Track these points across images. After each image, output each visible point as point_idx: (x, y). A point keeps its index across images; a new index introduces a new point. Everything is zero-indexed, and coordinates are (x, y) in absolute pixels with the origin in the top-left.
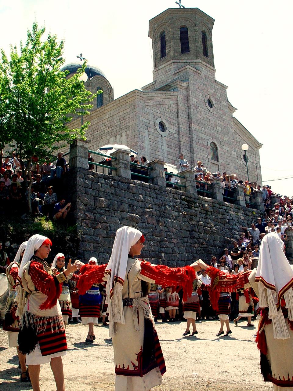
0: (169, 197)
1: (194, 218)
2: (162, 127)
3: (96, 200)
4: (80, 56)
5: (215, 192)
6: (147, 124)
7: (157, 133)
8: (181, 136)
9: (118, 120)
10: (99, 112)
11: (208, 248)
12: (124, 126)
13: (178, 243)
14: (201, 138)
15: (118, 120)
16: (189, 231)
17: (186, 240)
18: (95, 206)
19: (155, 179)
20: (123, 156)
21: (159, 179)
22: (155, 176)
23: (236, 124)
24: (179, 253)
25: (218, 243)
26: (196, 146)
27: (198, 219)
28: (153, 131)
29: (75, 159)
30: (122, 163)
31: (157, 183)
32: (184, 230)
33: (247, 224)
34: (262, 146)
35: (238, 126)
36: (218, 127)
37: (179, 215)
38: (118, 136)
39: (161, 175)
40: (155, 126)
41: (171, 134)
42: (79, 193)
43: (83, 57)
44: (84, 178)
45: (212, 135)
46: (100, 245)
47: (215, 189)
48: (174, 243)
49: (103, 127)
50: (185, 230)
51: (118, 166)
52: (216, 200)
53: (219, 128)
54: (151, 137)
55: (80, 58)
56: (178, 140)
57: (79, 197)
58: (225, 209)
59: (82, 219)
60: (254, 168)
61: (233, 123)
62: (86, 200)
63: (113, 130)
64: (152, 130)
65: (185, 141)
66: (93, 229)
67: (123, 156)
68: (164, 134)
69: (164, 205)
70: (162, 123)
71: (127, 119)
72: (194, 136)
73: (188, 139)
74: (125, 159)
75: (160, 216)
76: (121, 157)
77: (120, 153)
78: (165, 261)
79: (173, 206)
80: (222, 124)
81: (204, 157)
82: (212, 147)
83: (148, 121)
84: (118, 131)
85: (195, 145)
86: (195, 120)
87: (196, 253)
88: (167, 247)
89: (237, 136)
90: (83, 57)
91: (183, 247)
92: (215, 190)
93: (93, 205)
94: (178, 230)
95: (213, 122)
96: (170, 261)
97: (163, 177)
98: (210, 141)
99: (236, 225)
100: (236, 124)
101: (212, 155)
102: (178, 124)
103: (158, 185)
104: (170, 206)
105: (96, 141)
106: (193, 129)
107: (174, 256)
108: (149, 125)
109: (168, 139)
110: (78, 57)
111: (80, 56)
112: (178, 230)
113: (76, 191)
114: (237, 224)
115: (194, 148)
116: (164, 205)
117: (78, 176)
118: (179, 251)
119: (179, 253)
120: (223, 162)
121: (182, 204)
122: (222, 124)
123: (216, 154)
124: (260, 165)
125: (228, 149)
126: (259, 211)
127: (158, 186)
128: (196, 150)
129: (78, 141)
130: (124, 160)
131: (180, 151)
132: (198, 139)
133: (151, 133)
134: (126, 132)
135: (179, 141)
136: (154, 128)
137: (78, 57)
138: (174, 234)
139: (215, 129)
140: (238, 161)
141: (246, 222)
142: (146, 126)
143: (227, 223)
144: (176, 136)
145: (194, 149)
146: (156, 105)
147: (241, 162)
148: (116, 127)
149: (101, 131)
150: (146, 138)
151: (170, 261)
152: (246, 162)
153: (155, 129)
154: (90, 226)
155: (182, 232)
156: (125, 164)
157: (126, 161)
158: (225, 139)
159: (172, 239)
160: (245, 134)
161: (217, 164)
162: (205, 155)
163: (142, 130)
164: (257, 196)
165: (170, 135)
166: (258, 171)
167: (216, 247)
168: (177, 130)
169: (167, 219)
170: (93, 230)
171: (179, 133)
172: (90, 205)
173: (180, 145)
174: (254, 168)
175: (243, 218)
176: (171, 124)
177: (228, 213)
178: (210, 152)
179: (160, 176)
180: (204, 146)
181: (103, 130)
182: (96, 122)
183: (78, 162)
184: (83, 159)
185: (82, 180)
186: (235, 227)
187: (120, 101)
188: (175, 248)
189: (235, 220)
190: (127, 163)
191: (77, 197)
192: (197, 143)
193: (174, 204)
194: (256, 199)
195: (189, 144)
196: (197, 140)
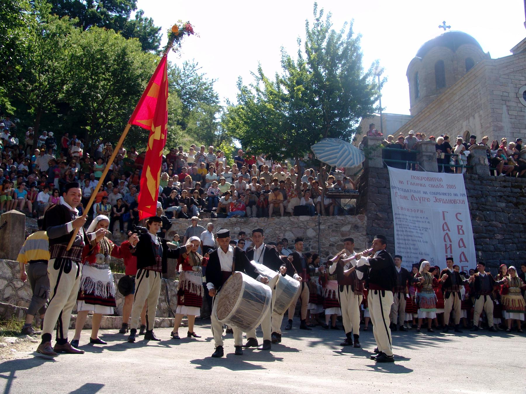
0: (494, 186)
4: (442, 25)
7: (522, 106)
9: (470, 100)
10: (448, 94)
13: (504, 239)
15: (470, 100)
17: (517, 235)
19: (474, 167)
21: (478, 168)
22: (474, 165)
24: (505, 251)
28: (515, 105)
30: (425, 155)
31: (476, 171)
32: (516, 223)
37: (507, 206)
38: (471, 119)
39: (482, 162)
43: (447, 25)
48: (498, 239)
49: (455, 111)
50: (517, 223)
55: (442, 27)
64: (513, 104)
69: (484, 196)
71: (479, 97)
74: (429, 151)
75: (478, 209)
76: (424, 149)
77: (423, 145)
78: (482, 260)
79: (499, 196)
83: (505, 94)
88: (487, 244)
90: (447, 25)
91: (513, 243)
94: (506, 224)
96: (490, 261)
97: (485, 165)
103: (476, 174)
104: (495, 197)
105: (449, 128)
107: (498, 254)
110: (440, 27)
111: (442, 25)
112: (506, 224)
116: (484, 196)
118: (505, 249)
119: (505, 251)
129: (369, 141)
130: (429, 152)
134: (479, 112)
137: (440, 27)
142: (503, 100)
146: (518, 71)
149: (453, 116)
150: (503, 115)
151: (490, 261)
153: (517, 102)
154: (382, 227)
156: (430, 156)
157: (430, 152)
159: (495, 235)
181: (455, 114)
182: (447, 106)
185: (374, 180)
187: (469, 77)
190: (432, 154)
193: (502, 194)
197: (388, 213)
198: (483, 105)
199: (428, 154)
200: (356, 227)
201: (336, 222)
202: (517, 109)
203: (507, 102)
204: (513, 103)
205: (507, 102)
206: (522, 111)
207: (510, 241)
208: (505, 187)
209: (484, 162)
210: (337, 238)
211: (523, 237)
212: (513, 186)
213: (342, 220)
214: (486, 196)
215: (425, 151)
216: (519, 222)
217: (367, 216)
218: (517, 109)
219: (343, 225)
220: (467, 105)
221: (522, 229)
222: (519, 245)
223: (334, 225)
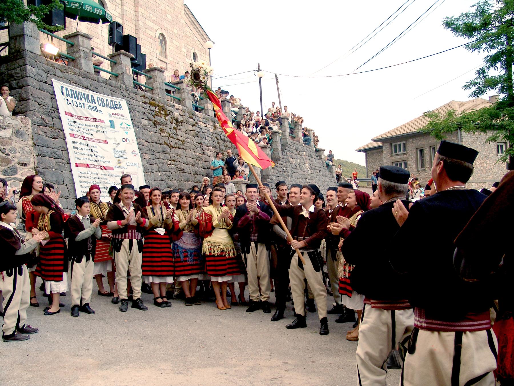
1: (165, 128)
3: (53, 100)
5: (183, 97)
11: (180, 166)
14: (148, 27)
16: (160, 144)
17: (158, 155)
18: (52, 107)
19: (120, 77)
20: (83, 41)
21: (125, 77)
25: (190, 160)
26: (143, 36)
27: (169, 130)
29: (22, 38)
31: (123, 81)
36: (168, 16)
39: (128, 72)
45: (161, 24)
46: (63, 161)
47: (184, 94)
50: (156, 143)
51: (76, 55)
52: (185, 108)
57: (32, 95)
58: (195, 119)
59: (38, 125)
61: (183, 12)
66: (53, 138)
67: (83, 41)
69: (132, 110)
72: (141, 23)
73: (133, 26)
74: (85, 46)
76: (81, 42)
77: (79, 37)
80: (172, 11)
81: (151, 52)
87: (169, 172)
89: (188, 29)
92: (183, 95)
95: (162, 8)
97: (130, 75)
98: (159, 32)
100: (187, 14)
101: (159, 49)
102: (122, 5)
103: (125, 85)
106: (140, 14)
114: (207, 137)
115: (140, 39)
120: (172, 59)
121: (152, 111)
122: (172, 11)
123: (164, 49)
125: (178, 44)
127: (125, 86)
130: (85, 47)
138: (146, 147)
139: (164, 17)
140: (187, 60)
141: (214, 135)
143: (198, 136)
145: (141, 40)
155: (154, 145)
157: (87, 48)
158: (175, 31)
159: (144, 154)
164: (225, 105)
167: (189, 165)
168: (121, 13)
169: (137, 129)
175: (212, 130)
176: (112, 3)
179: (126, 73)
180: (151, 38)
185: (34, 69)
188: (147, 165)
190: (88, 51)
193: (142, 110)
195: (135, 32)
196: (144, 29)
197: (53, 118)
199: (85, 49)
200: (18, 133)
207: (153, 161)
208: (145, 103)
209: (130, 72)
211: (162, 158)
212: (150, 104)
215: (82, 45)
216: (158, 142)
217: (32, 120)
221: (160, 150)
222: (160, 166)
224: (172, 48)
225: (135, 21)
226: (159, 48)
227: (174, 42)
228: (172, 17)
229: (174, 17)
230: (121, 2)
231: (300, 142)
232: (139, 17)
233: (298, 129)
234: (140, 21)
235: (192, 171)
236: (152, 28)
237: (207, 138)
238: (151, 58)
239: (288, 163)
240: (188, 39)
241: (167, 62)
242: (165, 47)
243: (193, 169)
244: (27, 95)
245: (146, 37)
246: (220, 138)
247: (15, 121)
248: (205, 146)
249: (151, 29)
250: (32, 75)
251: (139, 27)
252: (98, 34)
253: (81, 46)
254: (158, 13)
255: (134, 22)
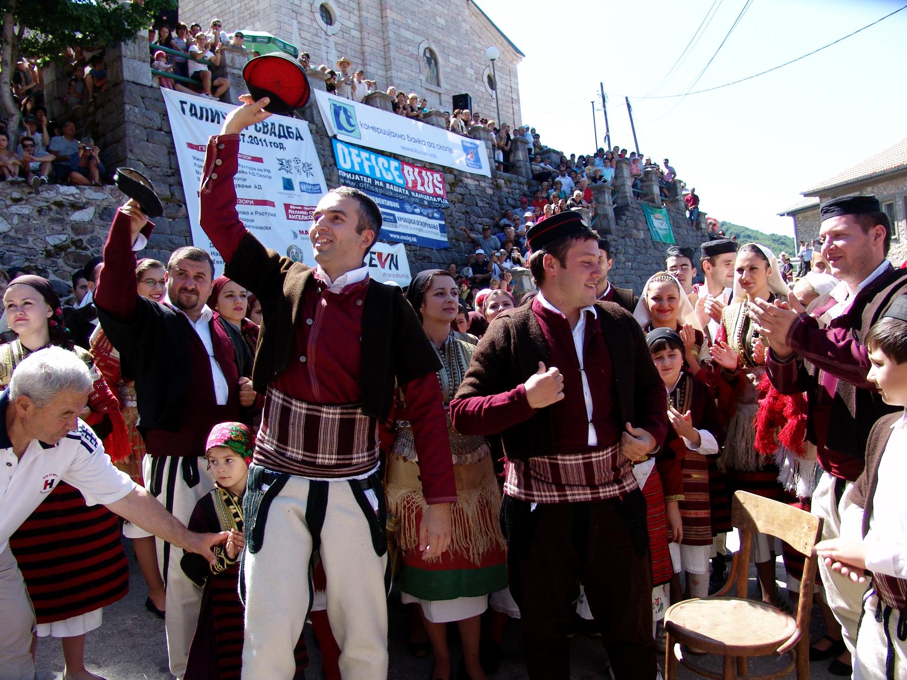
2: (327, 14)
3: (172, 157)
6: (296, 8)
7: (316, 26)
8: (366, 35)
12: (249, 12)
14: (405, 39)
23: (473, 14)
26: (397, 54)
28: (308, 23)
33: (499, 203)
34: (523, 59)
35: (476, 17)
36: (438, 19)
40: (311, 11)
41: (345, 31)
42: (132, 140)
44: (143, 105)
45: (427, 34)
53: (441, 21)
54: (304, 34)
56: (360, 43)
60: (508, 101)
62: (151, 156)
63: (227, 22)
64: (306, 21)
65: (373, 45)
67: (233, 60)
68: (330, 29)
69: (328, 165)
70: (326, 6)
72: (391, 35)
73: (379, 41)
77: (226, 52)
80: (446, 12)
82: (427, 58)
84: (237, 22)
85: (393, 53)
86: (393, 4)
89: (476, 38)
93: (168, 165)
95: (428, 8)
98: (424, 46)
99: (477, 205)
106: (390, 20)
108: (300, 11)
109: (340, 41)
113: (125, 135)
115: (392, 58)
116: (328, 165)
117: (126, 100)
120: (448, 87)
122: (446, 12)
124: (518, 95)
125: (459, 63)
126: (521, 178)
128: (396, 63)
130: (236, 68)
131: (364, 65)
132: (400, 42)
133: (305, 28)
134: (253, 24)
135: (362, 45)
136: (310, 17)
139: (433, 22)
140: (476, 86)
142: (293, 11)
144: (356, 34)
145: (393, 62)
147: (483, 89)
148: (232, 16)
150: (294, 36)
152: (492, 89)
153: (312, 20)
158: (453, 43)
160: (490, 35)
161: (437, 93)
162: (414, 74)
163: (285, 19)
164: (517, 148)
165: (343, 32)
166: (515, 106)
168: (358, 22)
170: (169, 222)
171: (361, 27)
172: (161, 166)
173: (363, 53)
174: (508, 101)
175: (490, 191)
176: (344, 9)
177: (461, 181)
178: (423, 67)
180: (411, 56)
183: (125, 70)
184: (136, 64)
185: (137, 110)
186: (476, 209)
189: (476, 196)
191: (128, 149)
192: (399, 49)
194: (515, 154)
196: (398, 44)
198: (262, 12)
201: (59, 198)
202: (313, 31)
203: (299, 16)
204: (307, 19)
205: (299, 16)
206: (317, 36)
210: (64, 237)
213: (73, 195)
214: (331, 165)
215: (231, 65)
218: (313, 31)
219: (76, 207)
220: (231, 10)
223: (54, 207)
224: (448, 70)
225: (383, 32)
226: (426, 70)
227: (451, 59)
228: (446, 21)
229: (449, 19)
230: (357, 5)
231: (654, 202)
232: (388, 25)
233: (651, 180)
234: (390, 32)
235: (445, 260)
236: (411, 41)
237: (480, 204)
238: (413, 88)
239: (627, 239)
240: (478, 54)
241: (440, 91)
242: (435, 70)
243: (449, 255)
244: (125, 151)
245: (402, 56)
246: (506, 203)
247: (99, 193)
248: (476, 218)
249: (410, 42)
250: (132, 118)
251: (389, 41)
252: (322, 58)
253: (229, 67)
254: (421, 16)
255: (380, 34)
